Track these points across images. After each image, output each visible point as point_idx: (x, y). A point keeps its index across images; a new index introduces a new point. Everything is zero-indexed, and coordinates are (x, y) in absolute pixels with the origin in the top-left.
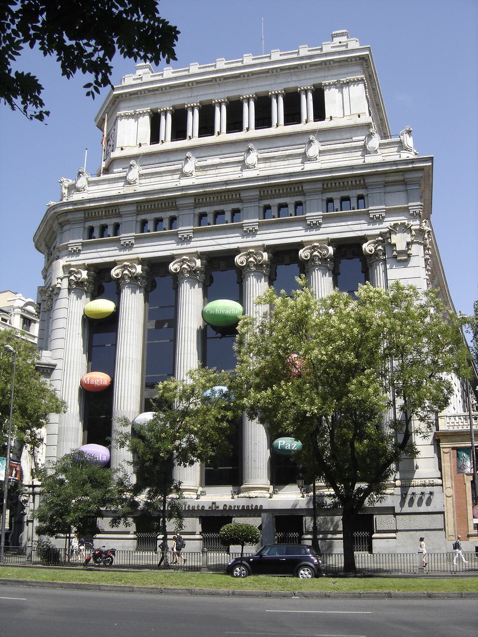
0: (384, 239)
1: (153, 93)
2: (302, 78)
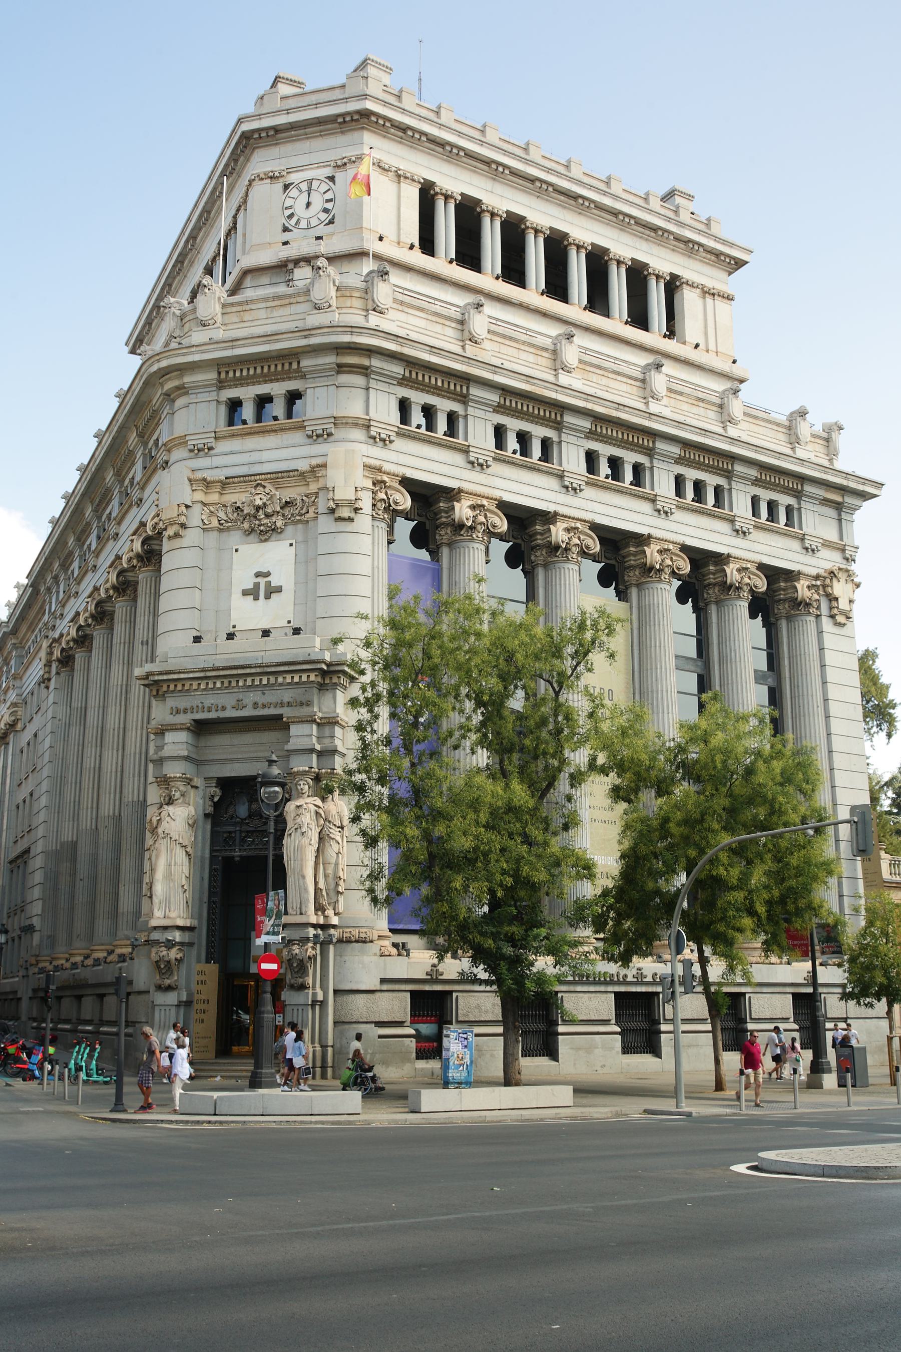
0: (823, 583)
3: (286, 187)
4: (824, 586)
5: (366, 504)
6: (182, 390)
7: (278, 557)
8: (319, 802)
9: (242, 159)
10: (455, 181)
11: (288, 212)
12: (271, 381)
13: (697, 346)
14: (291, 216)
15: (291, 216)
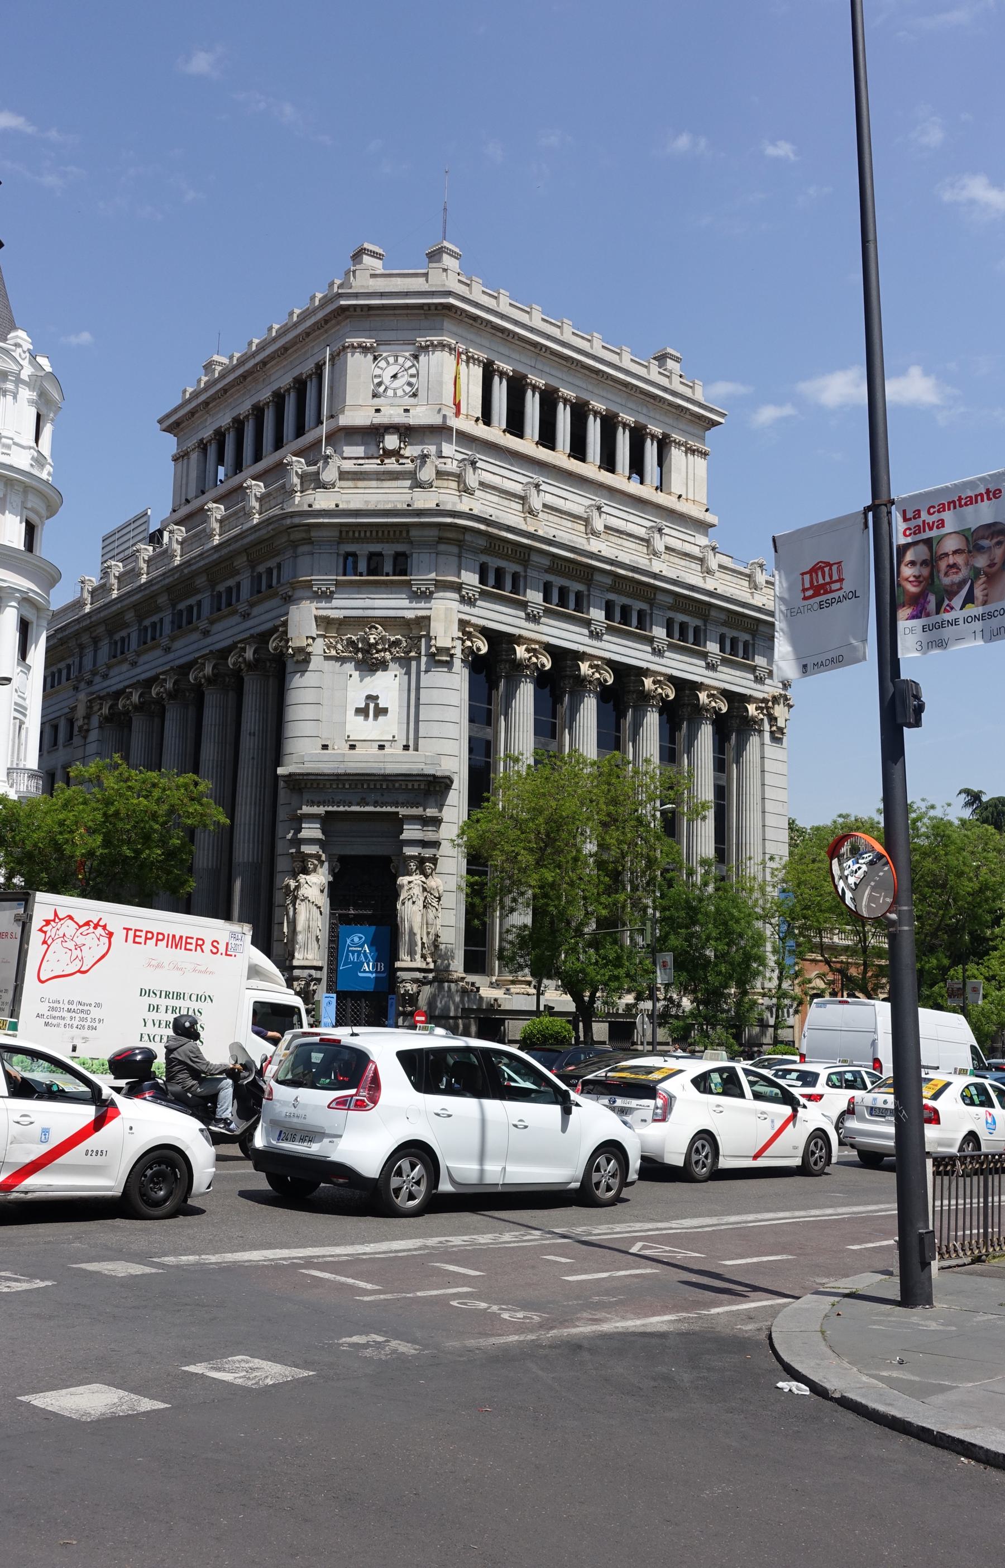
0: (766, 705)
1: (494, 331)
2: (652, 414)
3: (375, 358)
4: (768, 708)
5: (458, 652)
6: (309, 541)
7: (388, 685)
8: (424, 879)
9: (333, 322)
11: (376, 381)
12: (383, 542)
13: (680, 496)
14: (380, 384)
15: (380, 384)
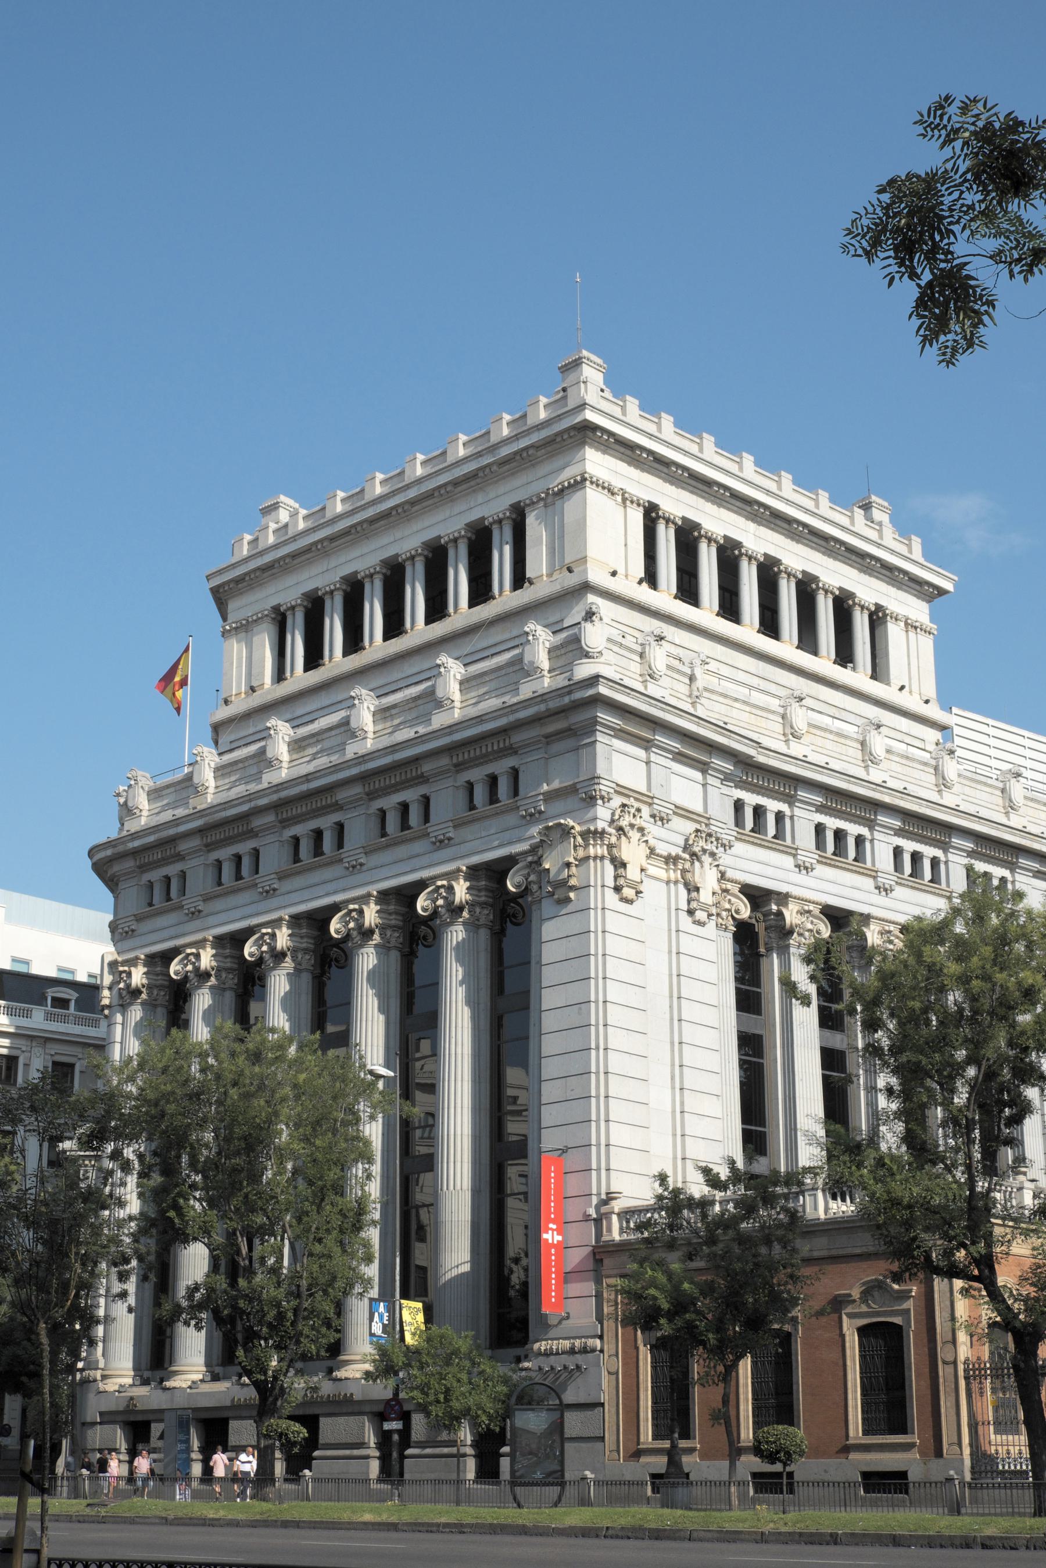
10: (678, 503)
13: (902, 688)
